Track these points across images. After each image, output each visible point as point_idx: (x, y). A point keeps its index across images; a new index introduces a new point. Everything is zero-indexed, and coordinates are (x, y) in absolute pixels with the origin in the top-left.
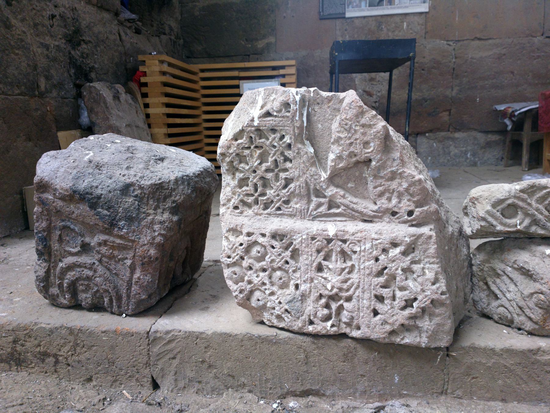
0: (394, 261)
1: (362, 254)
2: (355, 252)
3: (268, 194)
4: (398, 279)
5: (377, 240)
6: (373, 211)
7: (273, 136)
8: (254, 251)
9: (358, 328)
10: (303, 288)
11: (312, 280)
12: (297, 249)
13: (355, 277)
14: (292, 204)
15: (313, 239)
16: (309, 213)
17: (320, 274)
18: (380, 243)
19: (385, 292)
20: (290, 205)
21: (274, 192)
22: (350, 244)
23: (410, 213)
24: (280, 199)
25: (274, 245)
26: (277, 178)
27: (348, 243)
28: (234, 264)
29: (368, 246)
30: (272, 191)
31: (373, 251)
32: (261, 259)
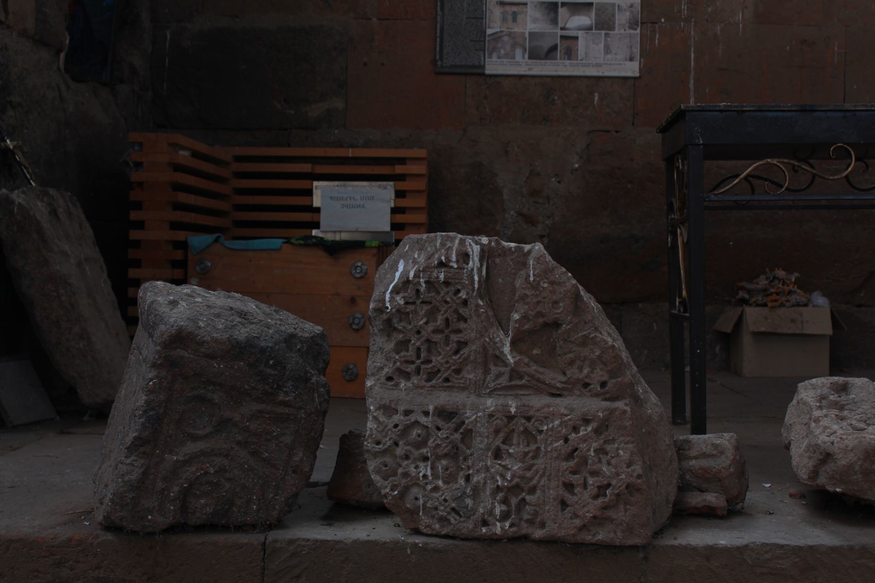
0: (585, 440)
1: (550, 433)
2: (541, 432)
3: (434, 360)
4: (590, 461)
5: (566, 415)
6: (562, 383)
7: (446, 290)
9: (543, 525)
12: (471, 431)
13: (540, 463)
14: (464, 374)
16: (485, 385)
18: (570, 420)
19: (574, 479)
20: (461, 376)
21: (442, 359)
22: (535, 422)
23: (603, 384)
24: (449, 368)
25: (440, 426)
26: (447, 341)
27: (533, 420)
28: (385, 452)
29: (557, 423)
30: (439, 358)
31: (562, 429)
32: (422, 443)
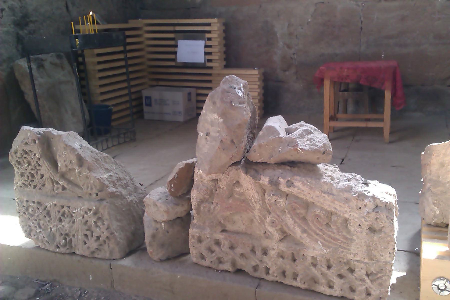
2: (74, 213)
8: (30, 210)
19: (88, 233)
29: (79, 209)
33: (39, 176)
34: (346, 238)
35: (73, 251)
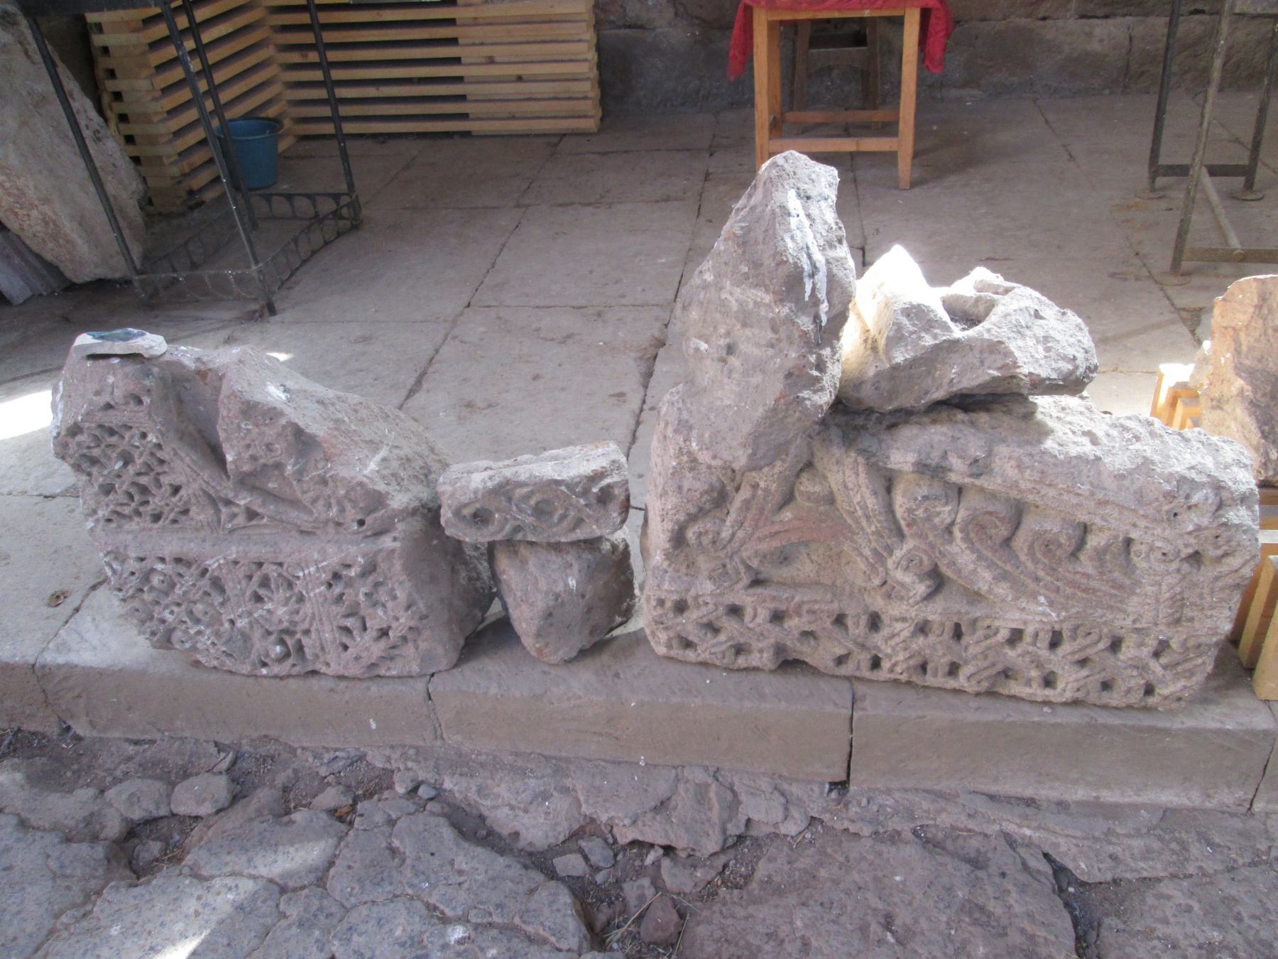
1: (308, 578)
2: (298, 578)
8: (156, 580)
10: (241, 623)
11: (250, 614)
15: (236, 563)
17: (259, 605)
19: (349, 622)
29: (312, 569)
30: (157, 500)
33: (166, 490)
34: (1121, 587)
35: (310, 669)
